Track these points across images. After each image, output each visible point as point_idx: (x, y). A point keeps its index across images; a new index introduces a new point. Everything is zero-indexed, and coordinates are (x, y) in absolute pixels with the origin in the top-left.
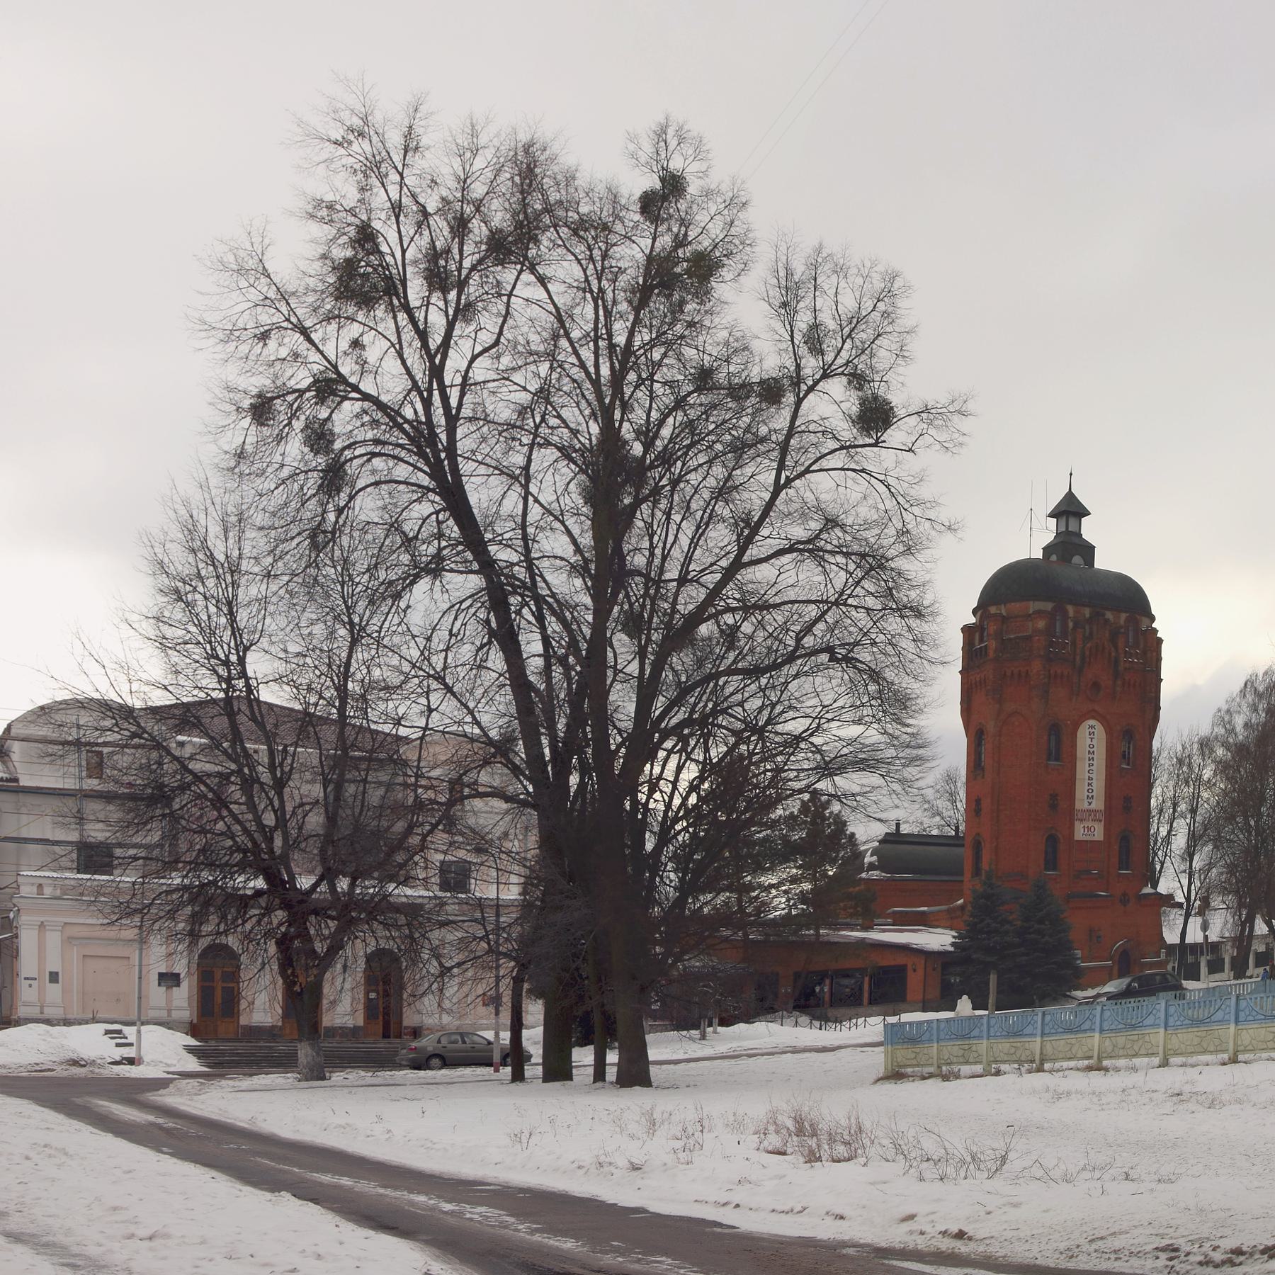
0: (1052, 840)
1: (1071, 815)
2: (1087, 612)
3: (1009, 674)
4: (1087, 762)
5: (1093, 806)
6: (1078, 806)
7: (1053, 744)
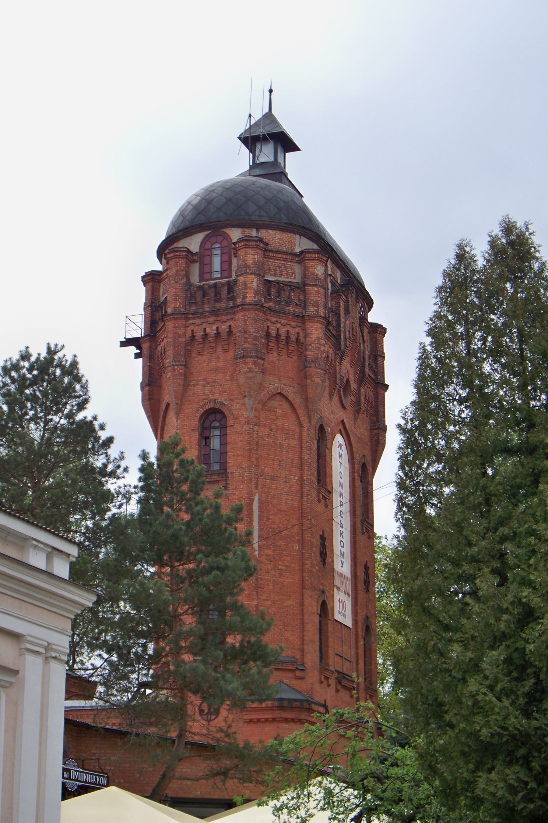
3: (273, 333)
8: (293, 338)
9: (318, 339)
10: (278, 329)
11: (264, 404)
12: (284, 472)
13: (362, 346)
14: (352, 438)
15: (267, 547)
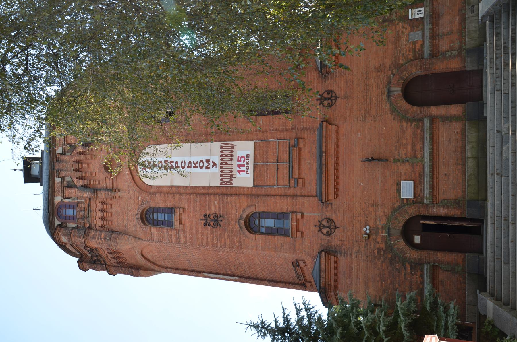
0: (250, 225)
1: (226, 192)
2: (58, 180)
3: (115, 261)
5: (217, 159)
6: (216, 183)
9: (97, 244)
11: (154, 263)
15: (230, 269)
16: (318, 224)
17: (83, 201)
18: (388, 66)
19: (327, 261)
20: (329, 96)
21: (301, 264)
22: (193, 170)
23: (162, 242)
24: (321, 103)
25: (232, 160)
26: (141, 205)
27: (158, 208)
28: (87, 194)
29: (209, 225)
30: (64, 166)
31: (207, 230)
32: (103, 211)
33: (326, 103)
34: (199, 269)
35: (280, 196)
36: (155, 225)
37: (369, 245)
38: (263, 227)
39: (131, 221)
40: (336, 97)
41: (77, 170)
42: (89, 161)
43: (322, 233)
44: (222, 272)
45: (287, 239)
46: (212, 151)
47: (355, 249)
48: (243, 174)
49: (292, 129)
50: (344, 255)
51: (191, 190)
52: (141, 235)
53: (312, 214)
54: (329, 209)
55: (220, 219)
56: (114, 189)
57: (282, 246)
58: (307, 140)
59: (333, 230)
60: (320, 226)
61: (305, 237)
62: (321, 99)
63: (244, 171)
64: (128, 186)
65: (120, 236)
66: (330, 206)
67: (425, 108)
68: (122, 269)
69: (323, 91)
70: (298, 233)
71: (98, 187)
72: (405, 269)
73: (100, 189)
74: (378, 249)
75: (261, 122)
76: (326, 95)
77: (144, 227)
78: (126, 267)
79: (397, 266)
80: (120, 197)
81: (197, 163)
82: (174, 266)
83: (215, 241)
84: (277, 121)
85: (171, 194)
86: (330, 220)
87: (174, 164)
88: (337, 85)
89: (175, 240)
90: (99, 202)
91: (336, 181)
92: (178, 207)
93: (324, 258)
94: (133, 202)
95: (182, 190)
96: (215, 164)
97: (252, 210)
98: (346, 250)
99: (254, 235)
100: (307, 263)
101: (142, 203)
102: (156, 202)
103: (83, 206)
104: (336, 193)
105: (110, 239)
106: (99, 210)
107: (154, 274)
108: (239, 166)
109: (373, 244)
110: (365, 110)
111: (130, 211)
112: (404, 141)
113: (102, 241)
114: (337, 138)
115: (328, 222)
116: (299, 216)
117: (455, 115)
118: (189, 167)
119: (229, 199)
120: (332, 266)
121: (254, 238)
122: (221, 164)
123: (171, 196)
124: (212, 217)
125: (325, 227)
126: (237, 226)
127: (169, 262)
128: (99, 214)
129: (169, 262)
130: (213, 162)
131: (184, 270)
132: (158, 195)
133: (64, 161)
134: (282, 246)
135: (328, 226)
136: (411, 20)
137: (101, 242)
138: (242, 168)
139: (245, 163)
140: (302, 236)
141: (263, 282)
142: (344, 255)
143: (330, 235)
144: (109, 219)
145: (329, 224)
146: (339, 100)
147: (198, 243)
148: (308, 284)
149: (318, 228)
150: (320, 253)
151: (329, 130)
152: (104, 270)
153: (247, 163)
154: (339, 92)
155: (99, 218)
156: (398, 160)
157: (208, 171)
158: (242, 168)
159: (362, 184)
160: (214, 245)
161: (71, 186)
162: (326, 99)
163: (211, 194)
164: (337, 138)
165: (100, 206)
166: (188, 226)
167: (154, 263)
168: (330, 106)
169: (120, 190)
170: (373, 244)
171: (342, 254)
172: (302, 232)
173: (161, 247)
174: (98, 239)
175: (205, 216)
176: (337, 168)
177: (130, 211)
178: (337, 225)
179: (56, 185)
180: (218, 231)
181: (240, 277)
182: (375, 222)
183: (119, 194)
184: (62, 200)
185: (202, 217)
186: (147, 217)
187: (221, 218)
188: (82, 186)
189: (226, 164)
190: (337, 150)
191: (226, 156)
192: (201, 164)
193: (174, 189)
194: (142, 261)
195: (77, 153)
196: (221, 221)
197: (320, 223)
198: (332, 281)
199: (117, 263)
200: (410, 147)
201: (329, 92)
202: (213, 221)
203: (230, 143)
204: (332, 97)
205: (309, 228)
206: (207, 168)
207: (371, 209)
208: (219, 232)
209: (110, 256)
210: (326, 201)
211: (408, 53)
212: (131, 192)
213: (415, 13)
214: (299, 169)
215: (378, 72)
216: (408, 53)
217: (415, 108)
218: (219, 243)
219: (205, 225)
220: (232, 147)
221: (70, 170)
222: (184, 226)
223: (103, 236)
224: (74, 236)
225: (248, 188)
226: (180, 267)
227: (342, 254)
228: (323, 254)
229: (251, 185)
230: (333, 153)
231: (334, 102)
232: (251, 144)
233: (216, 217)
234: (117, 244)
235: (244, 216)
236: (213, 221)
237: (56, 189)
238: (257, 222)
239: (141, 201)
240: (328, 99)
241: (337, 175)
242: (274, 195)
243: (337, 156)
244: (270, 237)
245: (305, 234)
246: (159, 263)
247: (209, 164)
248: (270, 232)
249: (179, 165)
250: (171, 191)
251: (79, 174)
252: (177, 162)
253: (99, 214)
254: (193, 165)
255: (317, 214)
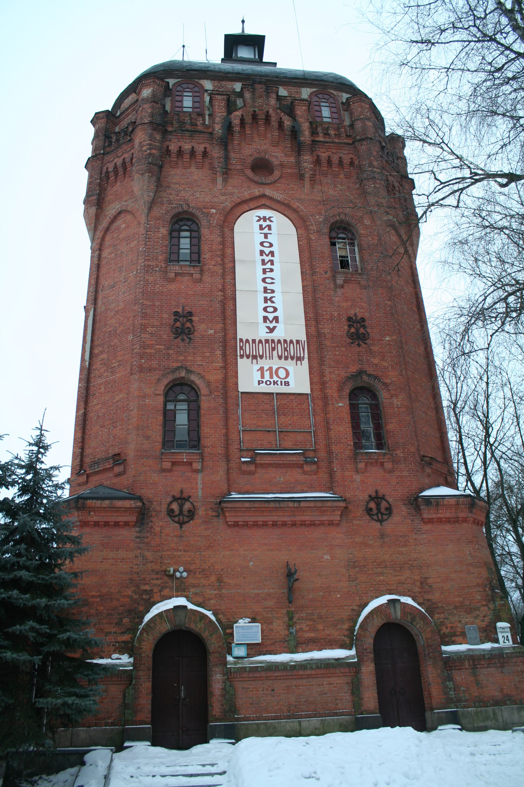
0: (180, 388)
1: (228, 347)
2: (238, 86)
3: (111, 169)
4: (260, 268)
5: (279, 334)
6: (242, 333)
7: (185, 243)
8: (128, 160)
9: (140, 143)
10: (116, 164)
11: (107, 230)
12: (124, 274)
13: (287, 122)
14: (296, 205)
15: (102, 352)
16: (185, 495)
17: (207, 123)
18: (429, 597)
19: (128, 510)
20: (383, 510)
21: (118, 469)
22: (261, 296)
23: (145, 244)
24: (371, 498)
25: (280, 358)
26: (203, 213)
27: (199, 238)
28: (218, 129)
29: (176, 321)
30: (261, 97)
31: (167, 317)
32: (193, 153)
33: (372, 505)
34: (99, 303)
35: (227, 435)
36: (171, 234)
37: (156, 576)
38: (175, 407)
39: (177, 195)
40: (381, 521)
41: (254, 116)
42: (269, 135)
43: (171, 502)
44: (96, 338)
45: (159, 445)
46: (293, 326)
47: (149, 555)
48: (257, 376)
49: (330, 452)
50: (138, 537)
51: (229, 292)
52: (157, 211)
53: (200, 486)
54: (210, 512)
55: (185, 338)
56: (227, 172)
57: (147, 438)
58: (315, 477)
59: (176, 519)
60: (181, 499)
61: (163, 474)
62: (377, 497)
63: (263, 376)
64: (232, 194)
65: (154, 179)
66: (214, 514)
67: (372, 655)
68: (97, 179)
69: (390, 500)
70: (170, 464)
71: (230, 147)
72: (123, 633)
73: (226, 150)
74: (152, 590)
75: (340, 404)
76: (384, 504)
77: (168, 217)
78: (100, 185)
79: (126, 620)
80: (214, 181)
81: (273, 302)
82: (104, 262)
83: (150, 330)
84: (343, 430)
85: (223, 260)
86: (192, 514)
87: (269, 266)
88: (400, 520)
89: (149, 266)
90: (205, 148)
91: (256, 524)
92: (202, 271)
93: (133, 506)
94: (207, 200)
95: (228, 279)
96: (271, 330)
97: (204, 390)
98: (146, 540)
99: (162, 393)
100: (120, 478)
101: (208, 214)
102: (210, 236)
103: (198, 123)
104: (236, 525)
105: (150, 163)
106: (193, 148)
107: (89, 230)
108: (270, 369)
109: (159, 582)
110: (364, 566)
111: (193, 195)
112: (320, 627)
113: (145, 151)
114: (322, 524)
115: (189, 511)
116: (197, 466)
117: (361, 699)
118: (265, 290)
119: (219, 353)
120: (120, 519)
121: (158, 392)
122: (273, 341)
123: (219, 259)
124: (188, 325)
125: (181, 506)
126: (175, 365)
127: (110, 254)
128: (187, 147)
129: (110, 254)
130: (275, 327)
131: (97, 278)
132: (219, 239)
133: (268, 97)
134: (147, 438)
135: (182, 511)
136: (495, 628)
137: (144, 148)
138: (267, 374)
139: (275, 378)
140: (164, 470)
141: (83, 406)
142: (138, 537)
143: (169, 514)
144: (180, 163)
145: (186, 513)
146: (378, 525)
147: (145, 302)
148: (83, 479)
149: (178, 495)
150: (140, 499)
151: (334, 511)
152: (94, 150)
153: (275, 383)
154: (389, 525)
155: (180, 147)
156: (291, 619)
157: (261, 320)
158: (267, 374)
159: (251, 564)
160: (144, 328)
161: (230, 107)
162: (378, 505)
163: (224, 324)
164: (322, 524)
165: (200, 149)
166: (173, 287)
167: (107, 230)
168: (369, 511)
169: (225, 180)
170: (159, 582)
171: (139, 535)
172: (170, 471)
173: (135, 242)
174: (150, 145)
175: (190, 314)
176: (275, 524)
177: (193, 195)
178: (185, 527)
179: (229, 83)
180: (166, 334)
181: (89, 369)
182: (194, 586)
183: (220, 180)
184: (206, 91)
185: (188, 309)
186: (184, 220)
187: (187, 340)
188: (230, 123)
189: (273, 349)
190: (303, 524)
191: (286, 349)
192: (270, 309)
193: (230, 265)
194: (111, 210)
195: (281, 118)
196: (183, 340)
197: (187, 499)
198: (95, 519)
199: (107, 172)
200: (312, 635)
201: (389, 510)
202: (182, 327)
203: (306, 356)
204: (382, 514)
205: (177, 482)
206: (265, 319)
207: (213, 578)
208: (165, 337)
209: (119, 161)
210: (222, 509)
211: (449, 625)
212: (223, 198)
213: (504, 632)
214: (270, 465)
215: (421, 583)
216: (449, 625)
217: (371, 641)
218: (147, 336)
219: (176, 313)
220: (300, 359)
221: (255, 107)
222: (171, 281)
223: (154, 151)
224: (152, 107)
225: (237, 384)
226: (103, 271)
227: (139, 535)
228: (139, 504)
229: (242, 388)
230: (298, 518)
231: (375, 517)
232: (306, 389)
233: (189, 331)
234: (142, 174)
235: (193, 377)
236: (182, 327)
237: (224, 83)
238: (182, 397)
239: (209, 213)
240: (378, 509)
241: (265, 524)
242: (226, 424)
243: (294, 524)
244: (160, 418)
245: (167, 474)
246: (108, 238)
247: (271, 321)
248: (169, 418)
249: (268, 274)
250: (226, 261)
251: (248, 119)
252: (272, 270)
253: (187, 147)
254: (269, 296)
255: (200, 493)
